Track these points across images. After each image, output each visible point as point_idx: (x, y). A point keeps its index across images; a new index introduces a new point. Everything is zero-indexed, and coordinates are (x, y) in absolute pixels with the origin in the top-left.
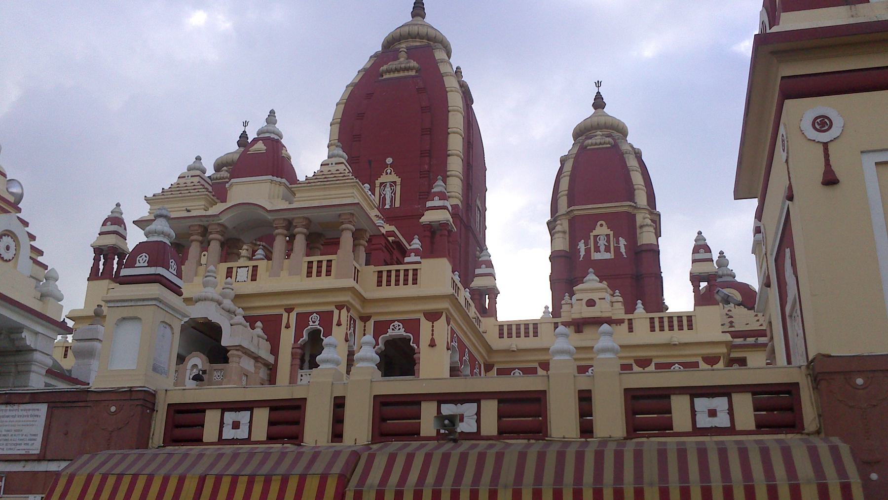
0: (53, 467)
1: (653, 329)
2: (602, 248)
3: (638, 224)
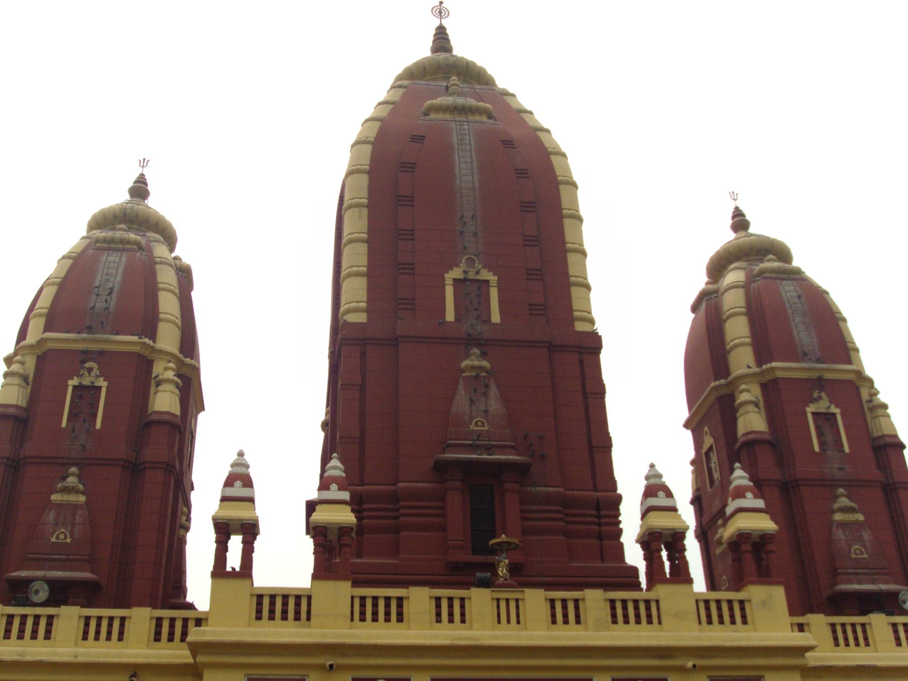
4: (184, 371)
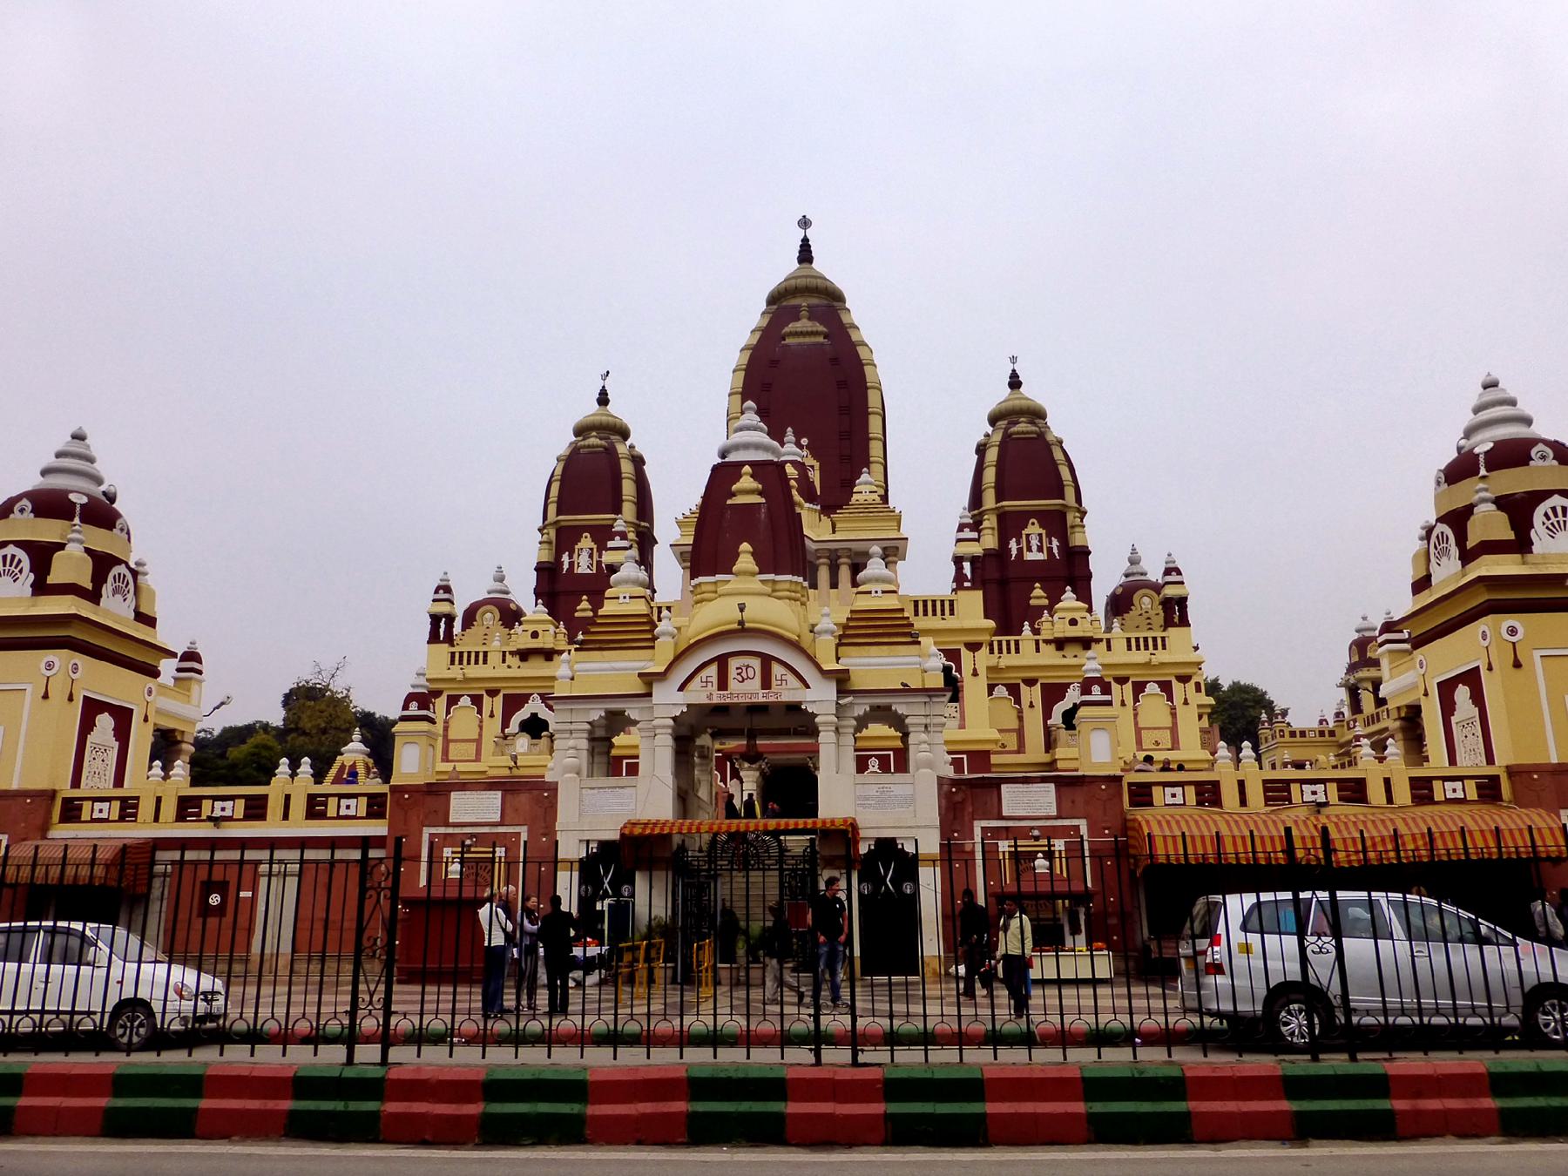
1: (1129, 648)
2: (1034, 548)
3: (1069, 523)
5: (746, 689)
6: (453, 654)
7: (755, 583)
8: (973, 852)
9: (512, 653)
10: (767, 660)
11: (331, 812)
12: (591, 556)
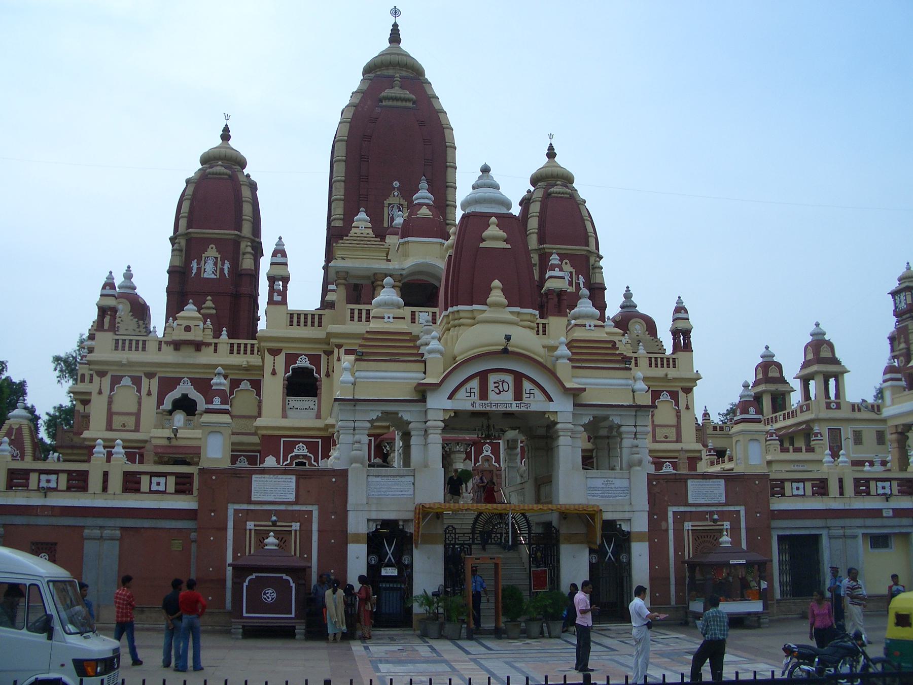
0: (731, 508)
1: (650, 365)
4: (255, 244)
5: (502, 399)
6: (117, 341)
7: (507, 314)
8: (667, 530)
9: (167, 343)
10: (519, 378)
11: (144, 486)
12: (215, 264)
